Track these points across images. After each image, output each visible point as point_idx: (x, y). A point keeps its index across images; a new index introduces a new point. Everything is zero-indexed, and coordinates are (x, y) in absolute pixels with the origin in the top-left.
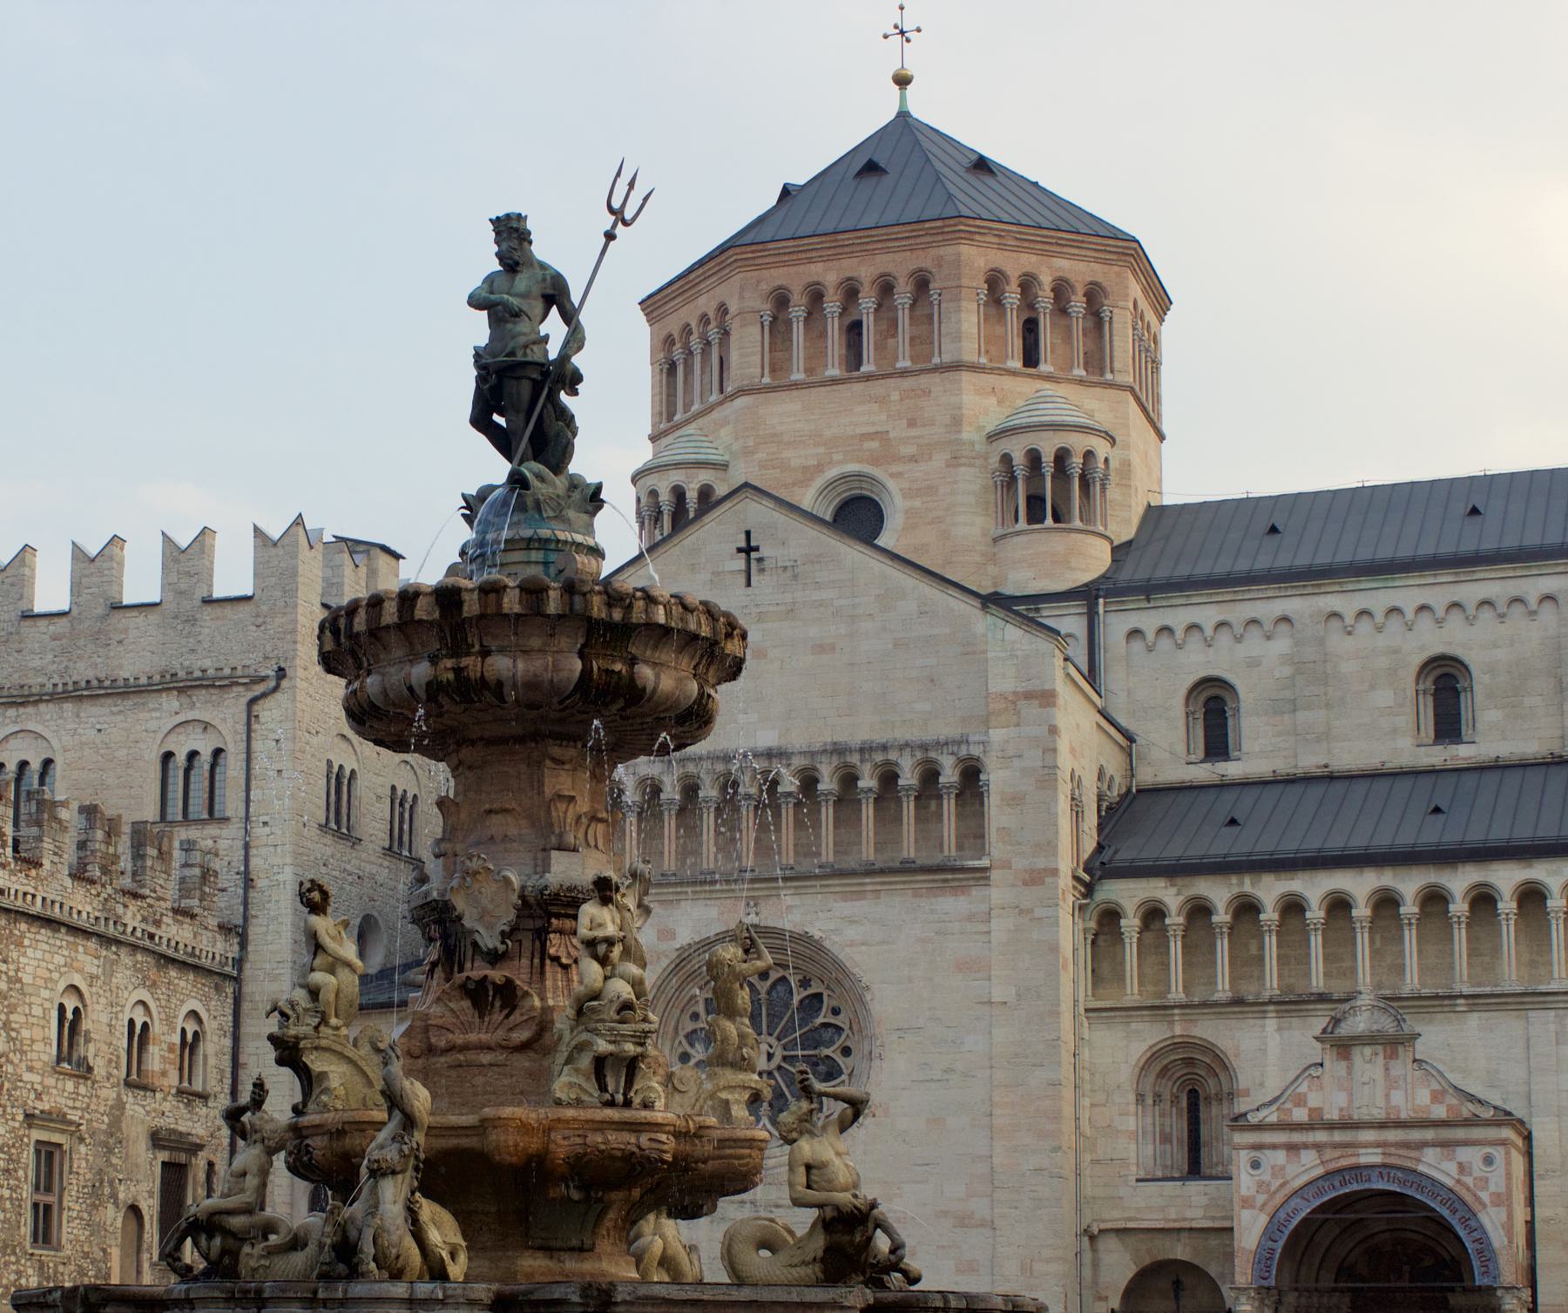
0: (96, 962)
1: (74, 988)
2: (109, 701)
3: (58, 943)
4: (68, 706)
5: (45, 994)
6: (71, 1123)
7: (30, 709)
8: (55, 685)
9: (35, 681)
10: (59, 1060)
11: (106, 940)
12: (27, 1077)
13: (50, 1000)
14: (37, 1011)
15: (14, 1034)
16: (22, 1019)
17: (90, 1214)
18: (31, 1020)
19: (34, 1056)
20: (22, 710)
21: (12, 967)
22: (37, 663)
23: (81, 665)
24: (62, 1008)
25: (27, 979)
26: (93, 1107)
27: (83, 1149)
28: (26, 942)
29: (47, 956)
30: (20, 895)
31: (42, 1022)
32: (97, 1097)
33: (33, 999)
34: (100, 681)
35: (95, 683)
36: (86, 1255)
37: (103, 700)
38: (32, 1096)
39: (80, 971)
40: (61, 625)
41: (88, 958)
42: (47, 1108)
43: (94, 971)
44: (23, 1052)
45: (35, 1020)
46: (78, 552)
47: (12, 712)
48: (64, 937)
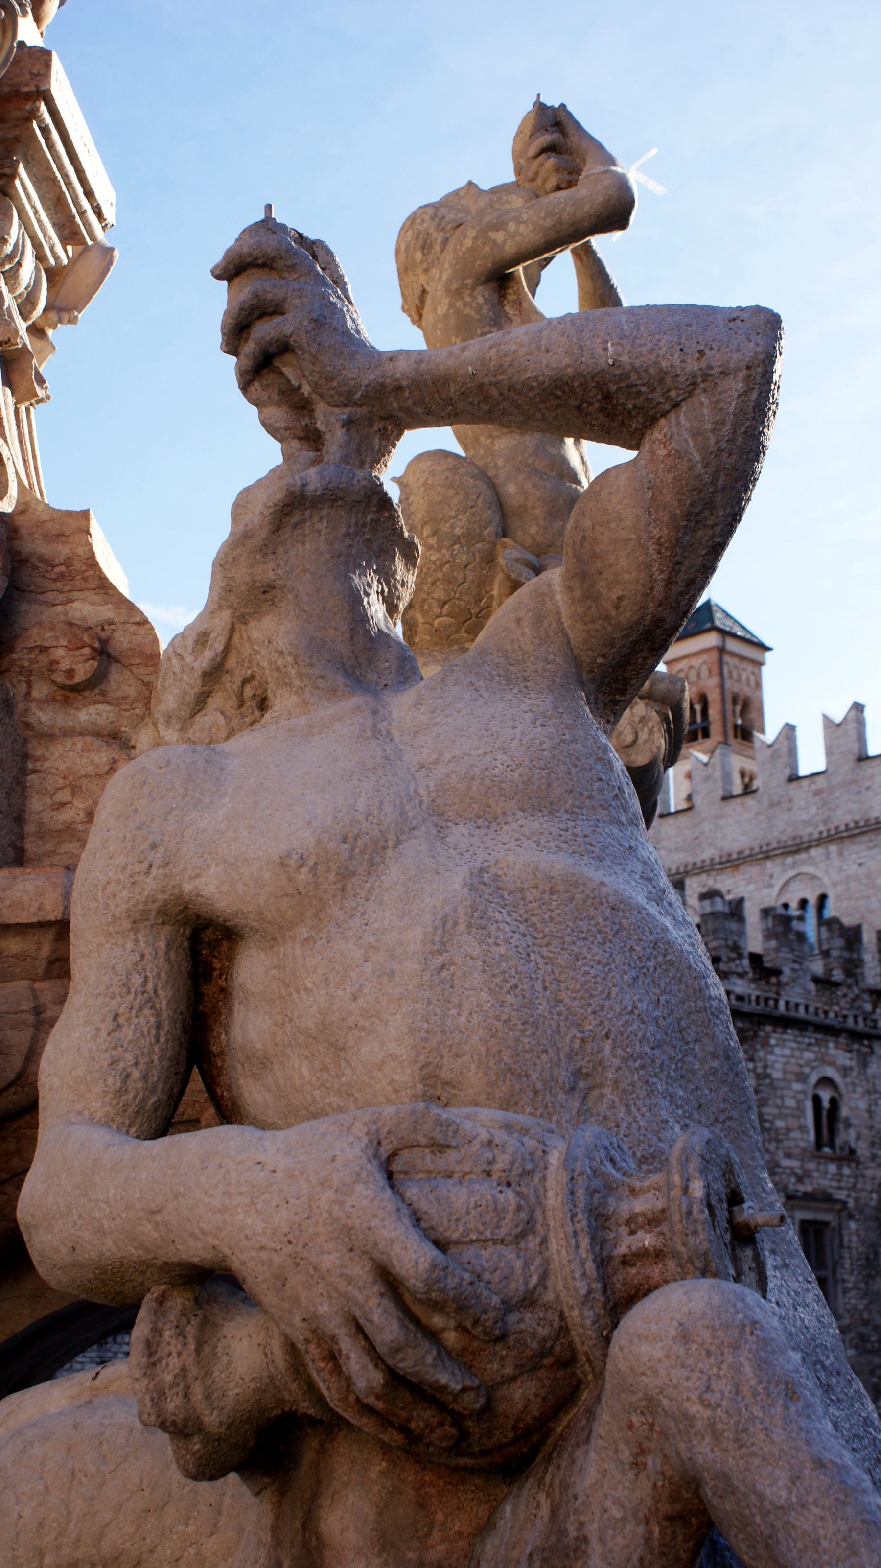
0: (848, 1055)
1: (826, 1081)
2: (865, 838)
3: (806, 1040)
4: (833, 848)
5: (797, 1086)
6: (837, 1201)
7: (803, 856)
8: (821, 832)
9: (805, 832)
10: (819, 1145)
11: (855, 1036)
12: (786, 1162)
13: (804, 1092)
14: (790, 1103)
15: (767, 1125)
16: (775, 1111)
17: (867, 1284)
18: (784, 1111)
19: (792, 1143)
20: (797, 857)
21: (760, 1065)
22: (804, 817)
23: (839, 812)
24: (817, 1100)
25: (777, 1075)
26: (859, 1186)
27: (853, 1225)
28: (773, 1042)
29: (797, 1053)
30: (762, 1001)
31: (796, 1113)
32: (863, 1176)
33: (785, 1092)
34: (856, 823)
35: (852, 825)
36: (866, 1323)
37: (859, 839)
38: (793, 1180)
39: (832, 1064)
40: (821, 782)
41: (839, 1054)
42: (809, 1188)
43: (848, 1063)
44: (778, 1141)
45: (789, 1111)
46: (828, 722)
47: (789, 860)
48: (810, 1037)
